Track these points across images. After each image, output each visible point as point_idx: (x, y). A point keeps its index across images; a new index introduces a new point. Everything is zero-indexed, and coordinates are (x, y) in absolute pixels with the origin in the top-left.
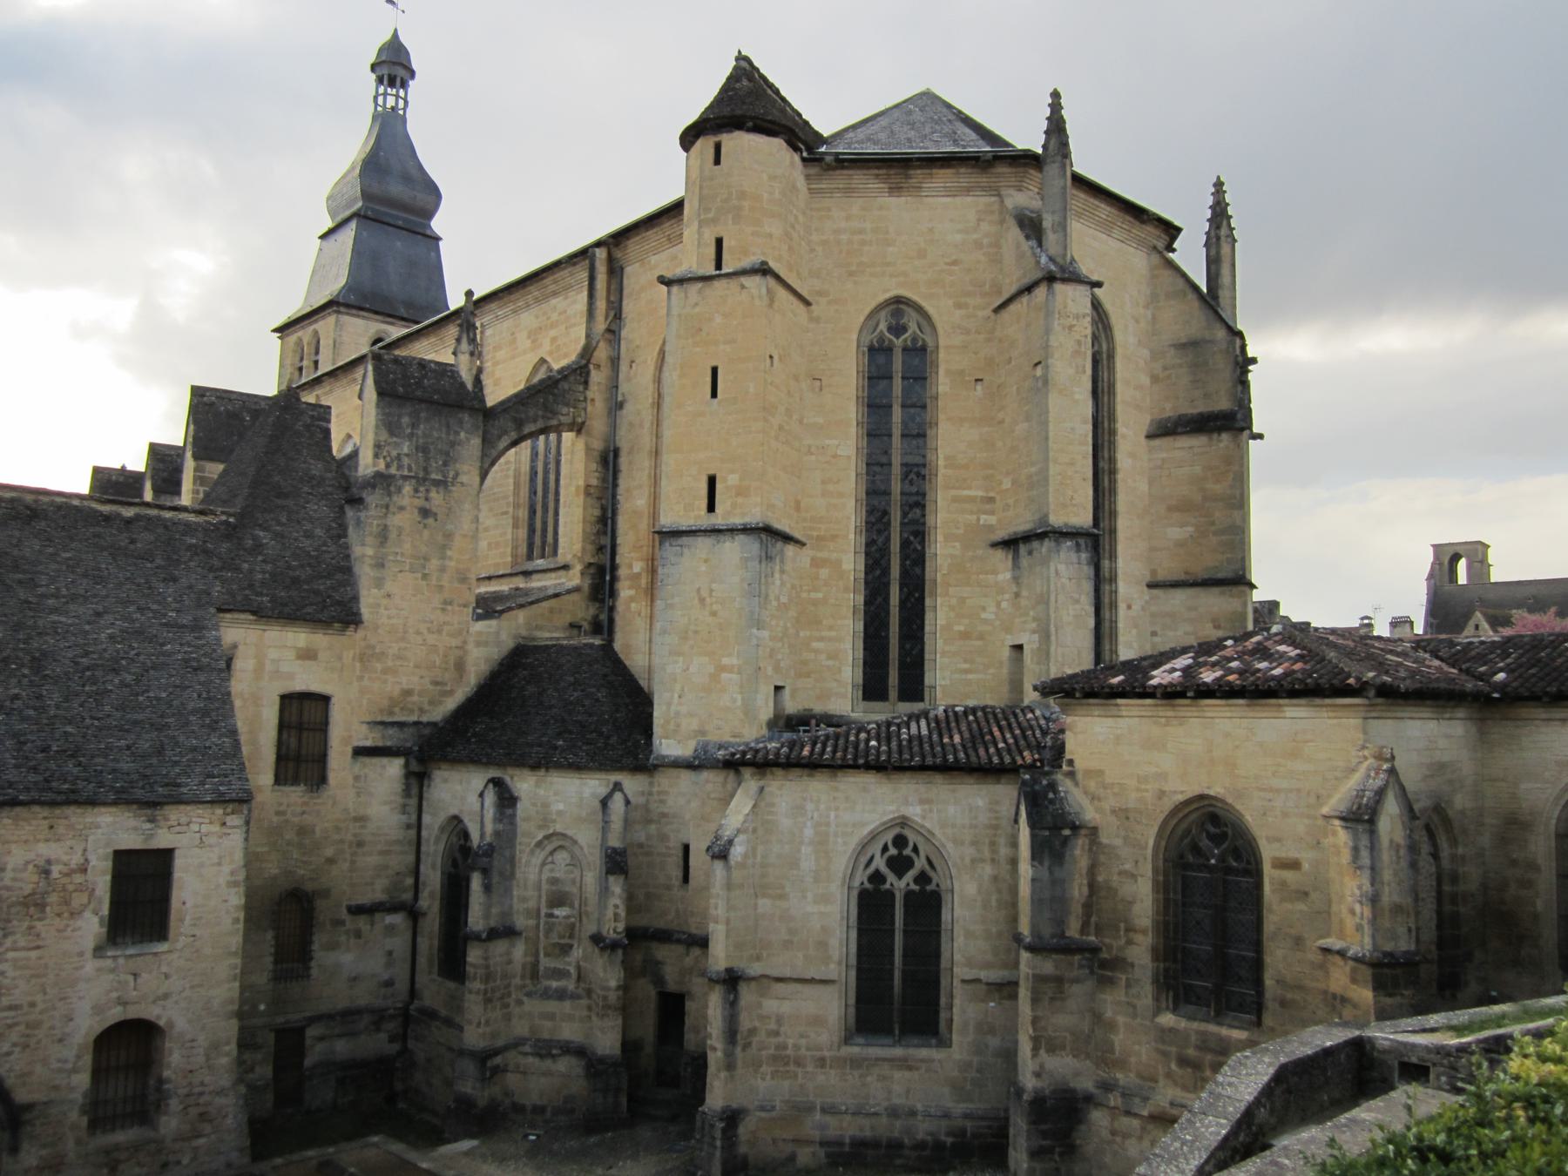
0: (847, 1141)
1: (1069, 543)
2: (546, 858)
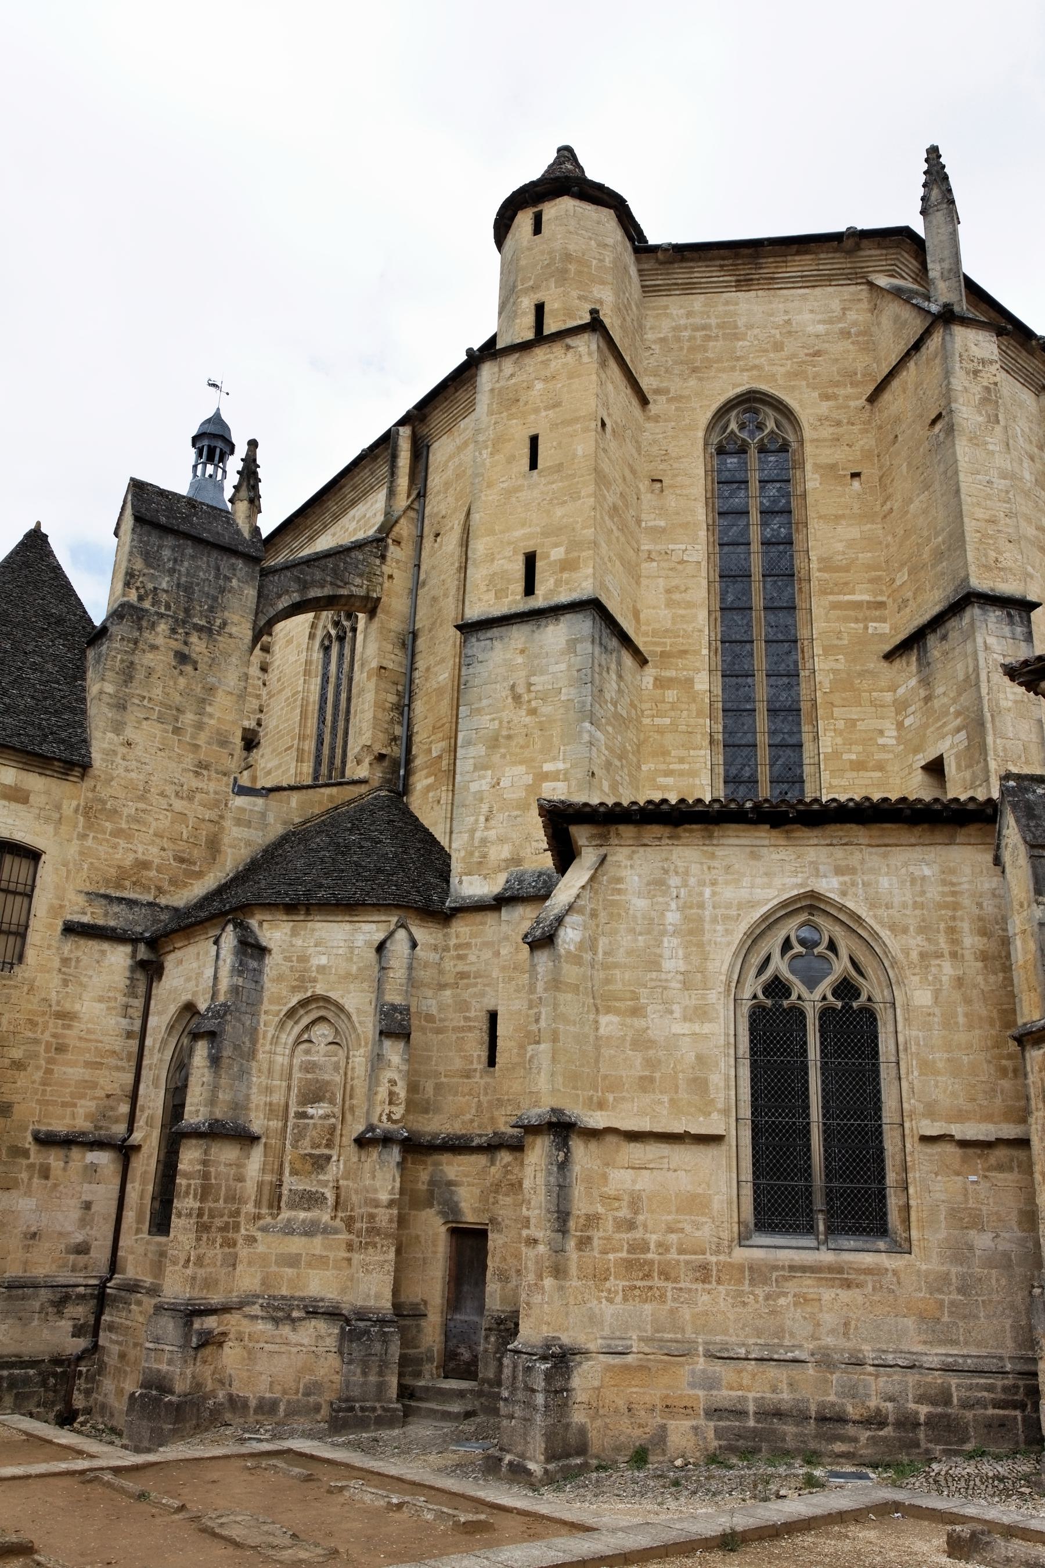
0: (751, 1408)
1: (998, 613)
2: (300, 1035)
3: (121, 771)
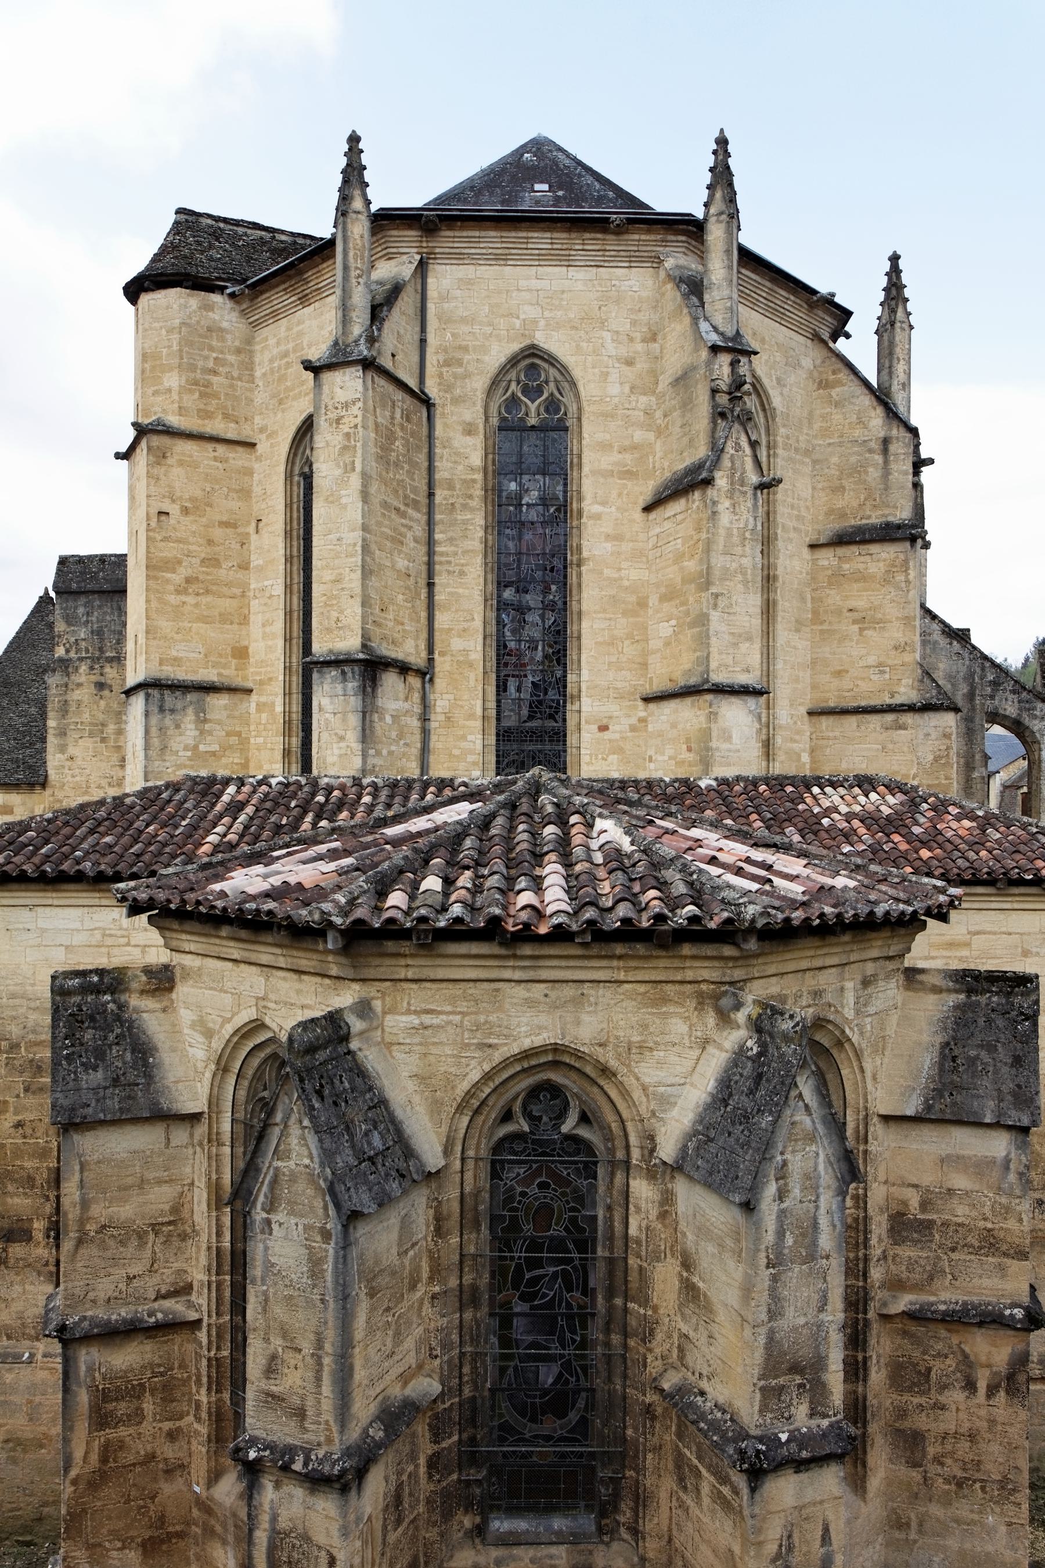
1: (333, 673)
3: (69, 778)
